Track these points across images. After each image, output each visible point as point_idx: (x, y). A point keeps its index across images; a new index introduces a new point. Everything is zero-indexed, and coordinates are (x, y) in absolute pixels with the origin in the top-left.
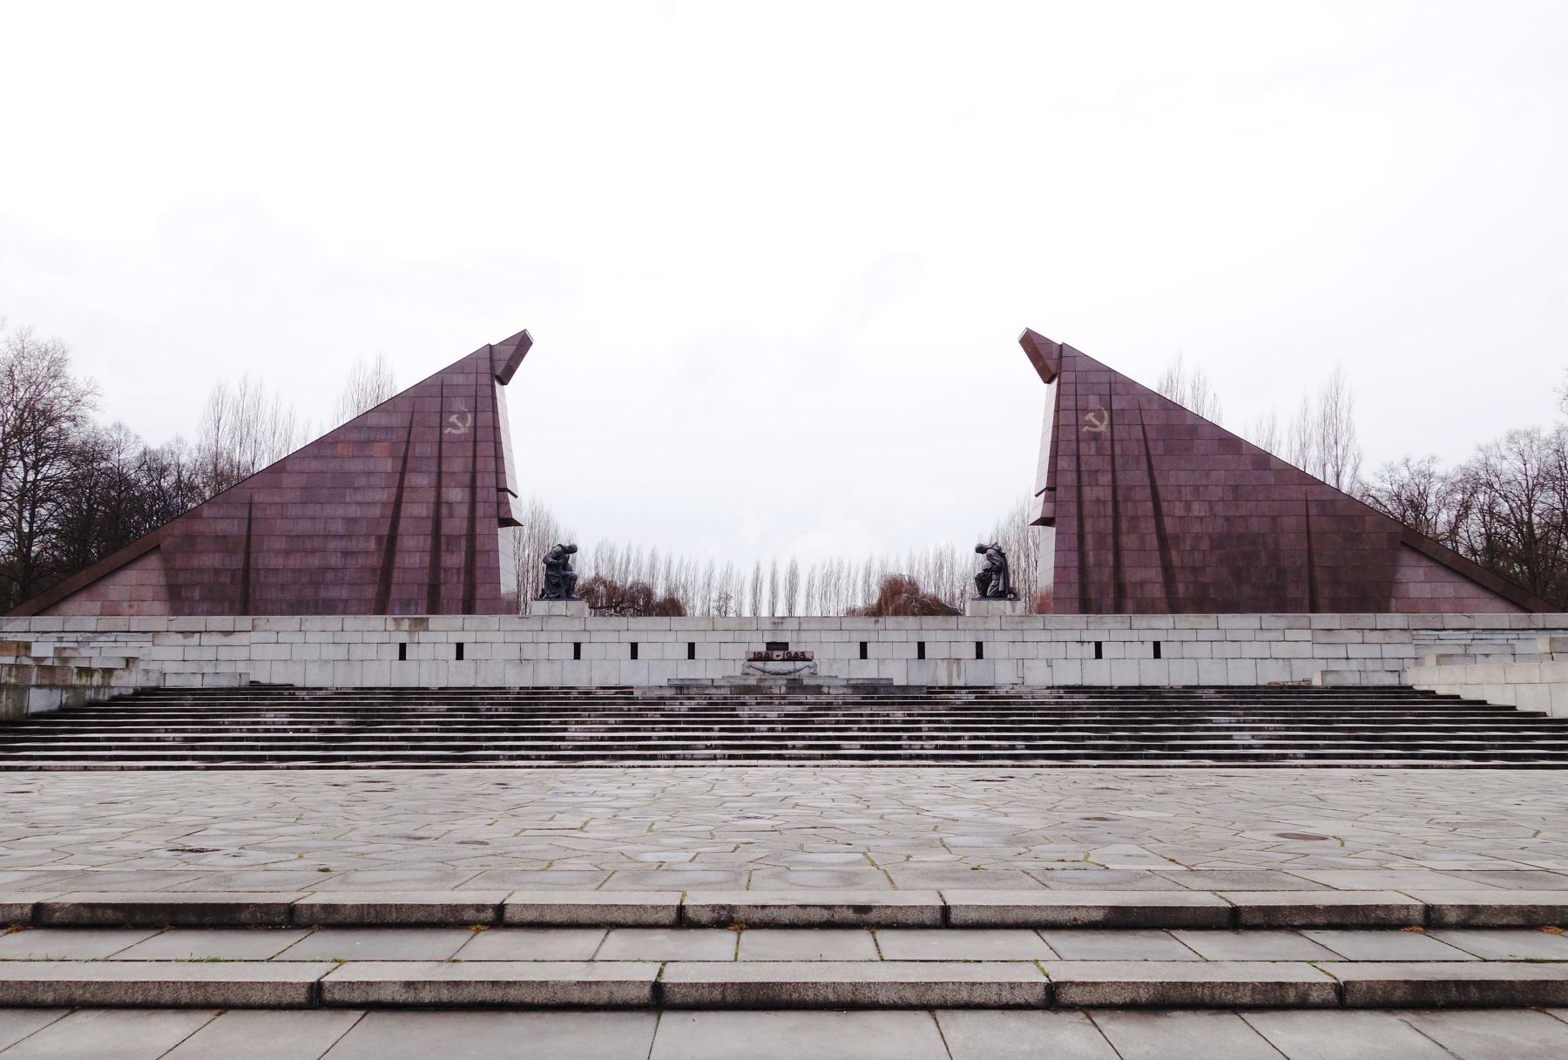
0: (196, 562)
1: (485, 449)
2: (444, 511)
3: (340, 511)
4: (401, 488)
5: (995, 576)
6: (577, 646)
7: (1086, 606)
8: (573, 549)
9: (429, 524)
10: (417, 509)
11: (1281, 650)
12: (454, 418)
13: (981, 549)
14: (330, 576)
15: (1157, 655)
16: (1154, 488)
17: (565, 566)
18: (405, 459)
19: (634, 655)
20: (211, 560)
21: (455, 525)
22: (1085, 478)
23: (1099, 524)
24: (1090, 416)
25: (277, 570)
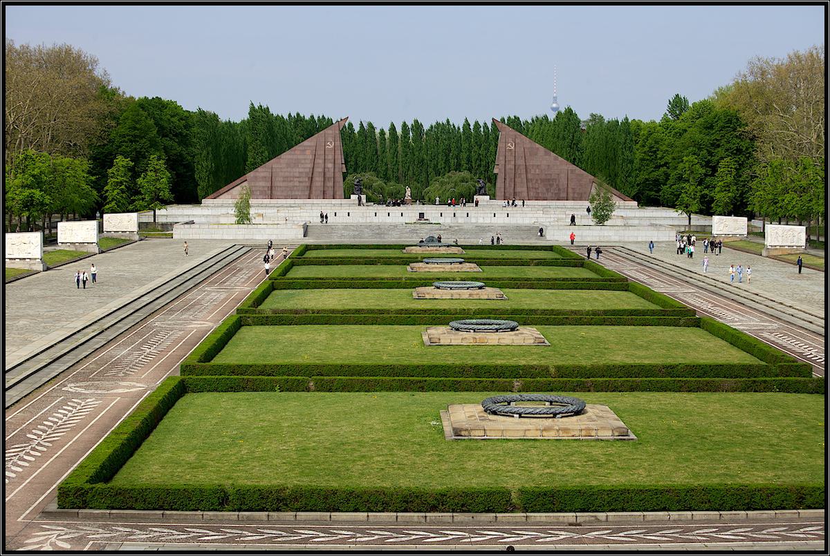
0: (257, 184)
2: (326, 170)
3: (297, 170)
10: (319, 170)
14: (295, 188)
20: (262, 184)
21: (330, 174)
23: (510, 175)
25: (280, 187)
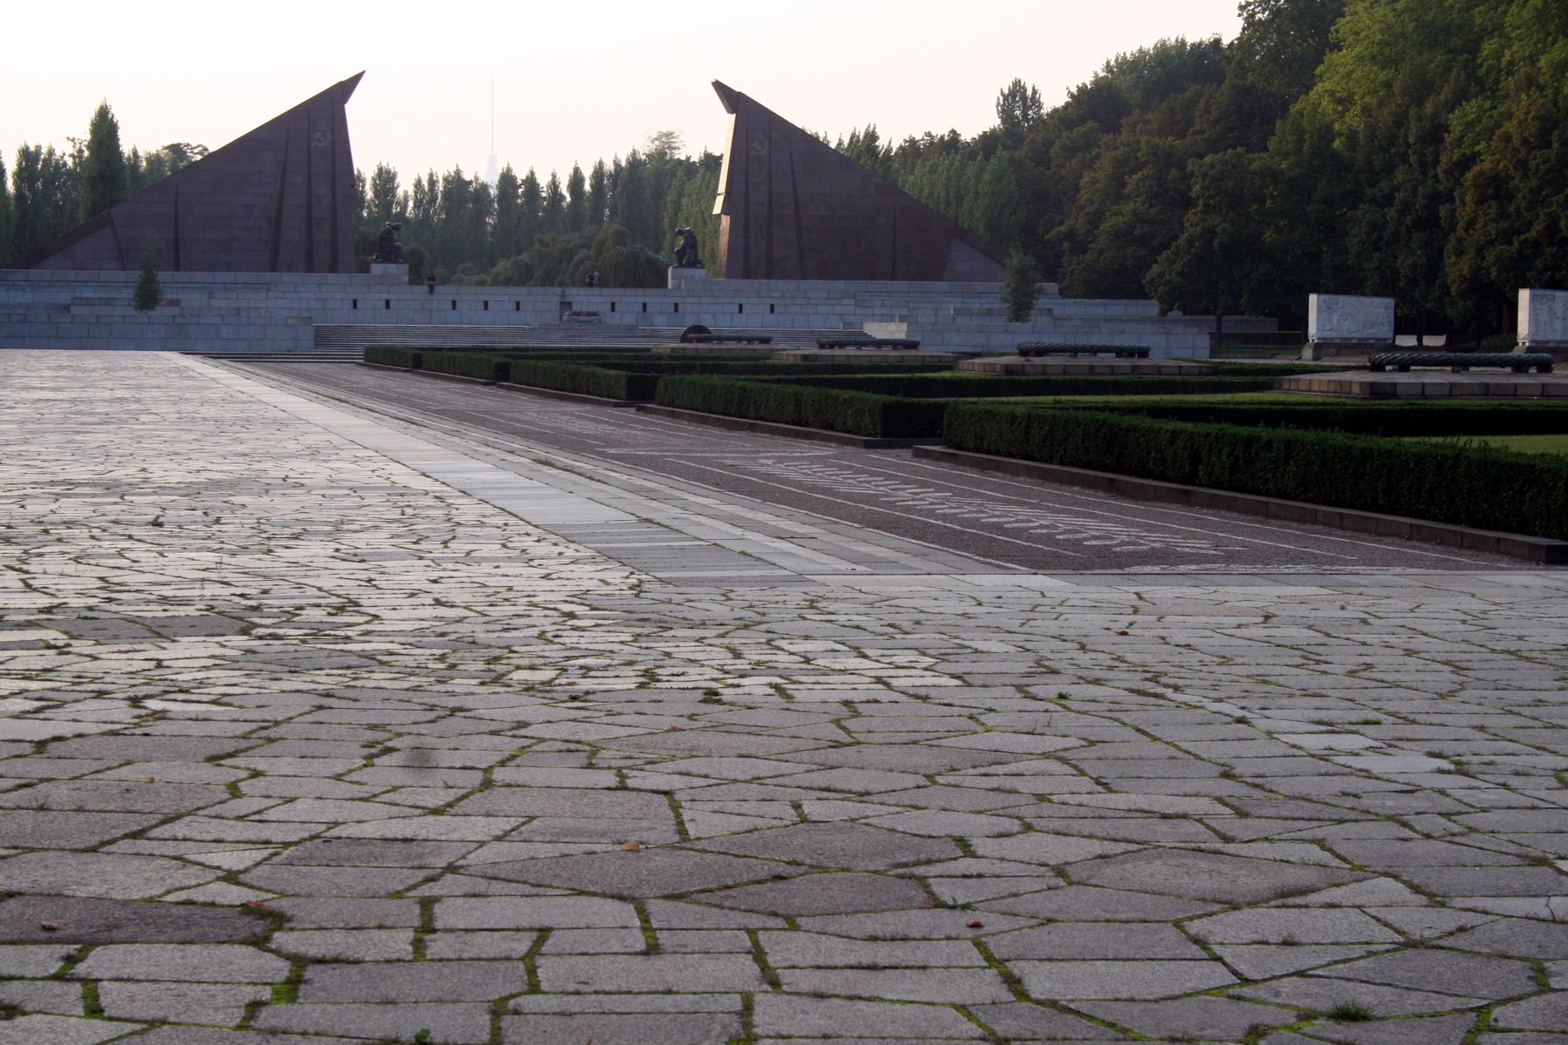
6: (454, 303)
7: (747, 274)
11: (839, 309)
12: (318, 135)
15: (772, 311)
19: (486, 308)
24: (756, 144)
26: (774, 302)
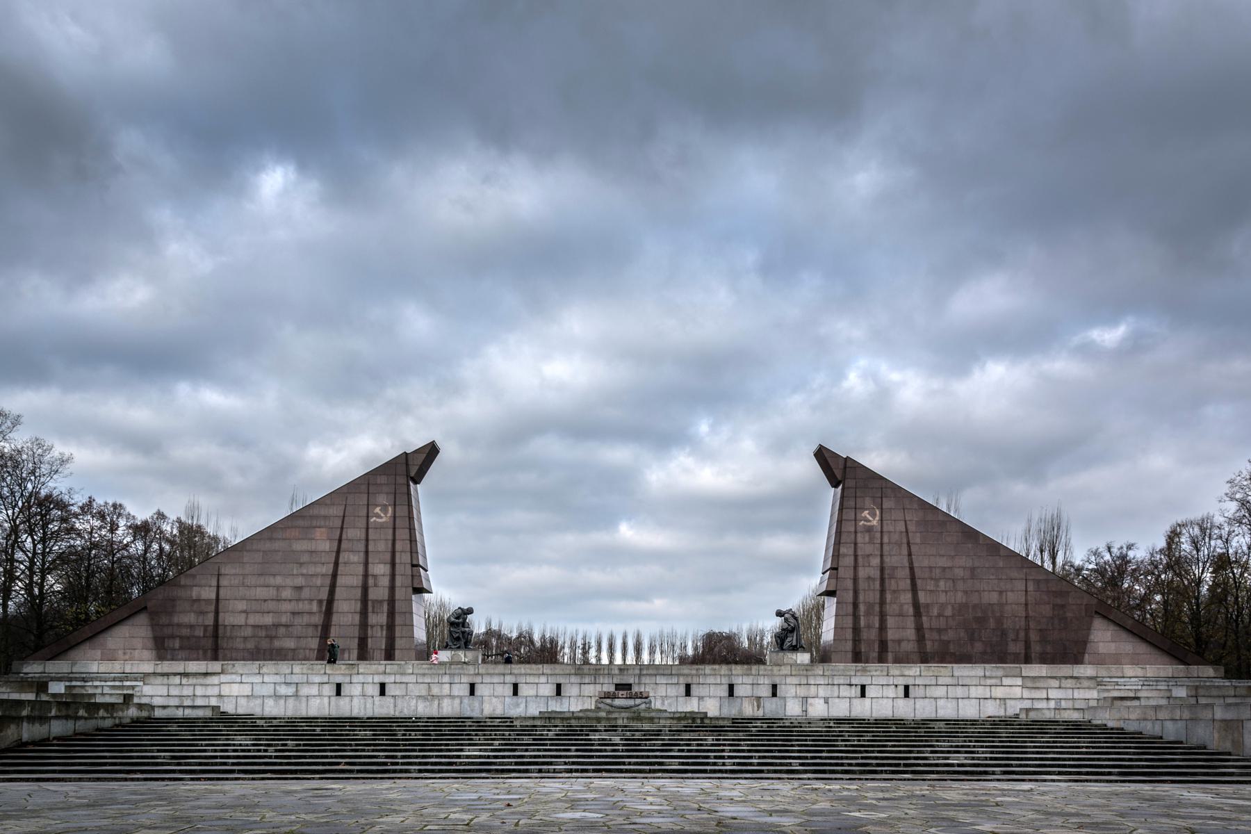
1: (402, 534)
2: (371, 581)
4: (336, 564)
5: (792, 633)
8: (470, 611)
9: (359, 593)
10: (350, 579)
11: (999, 692)
13: (779, 614)
14: (282, 631)
15: (907, 695)
16: (912, 569)
17: (464, 624)
18: (340, 541)
21: (379, 592)
22: (860, 560)
23: (869, 596)
26: (910, 682)
